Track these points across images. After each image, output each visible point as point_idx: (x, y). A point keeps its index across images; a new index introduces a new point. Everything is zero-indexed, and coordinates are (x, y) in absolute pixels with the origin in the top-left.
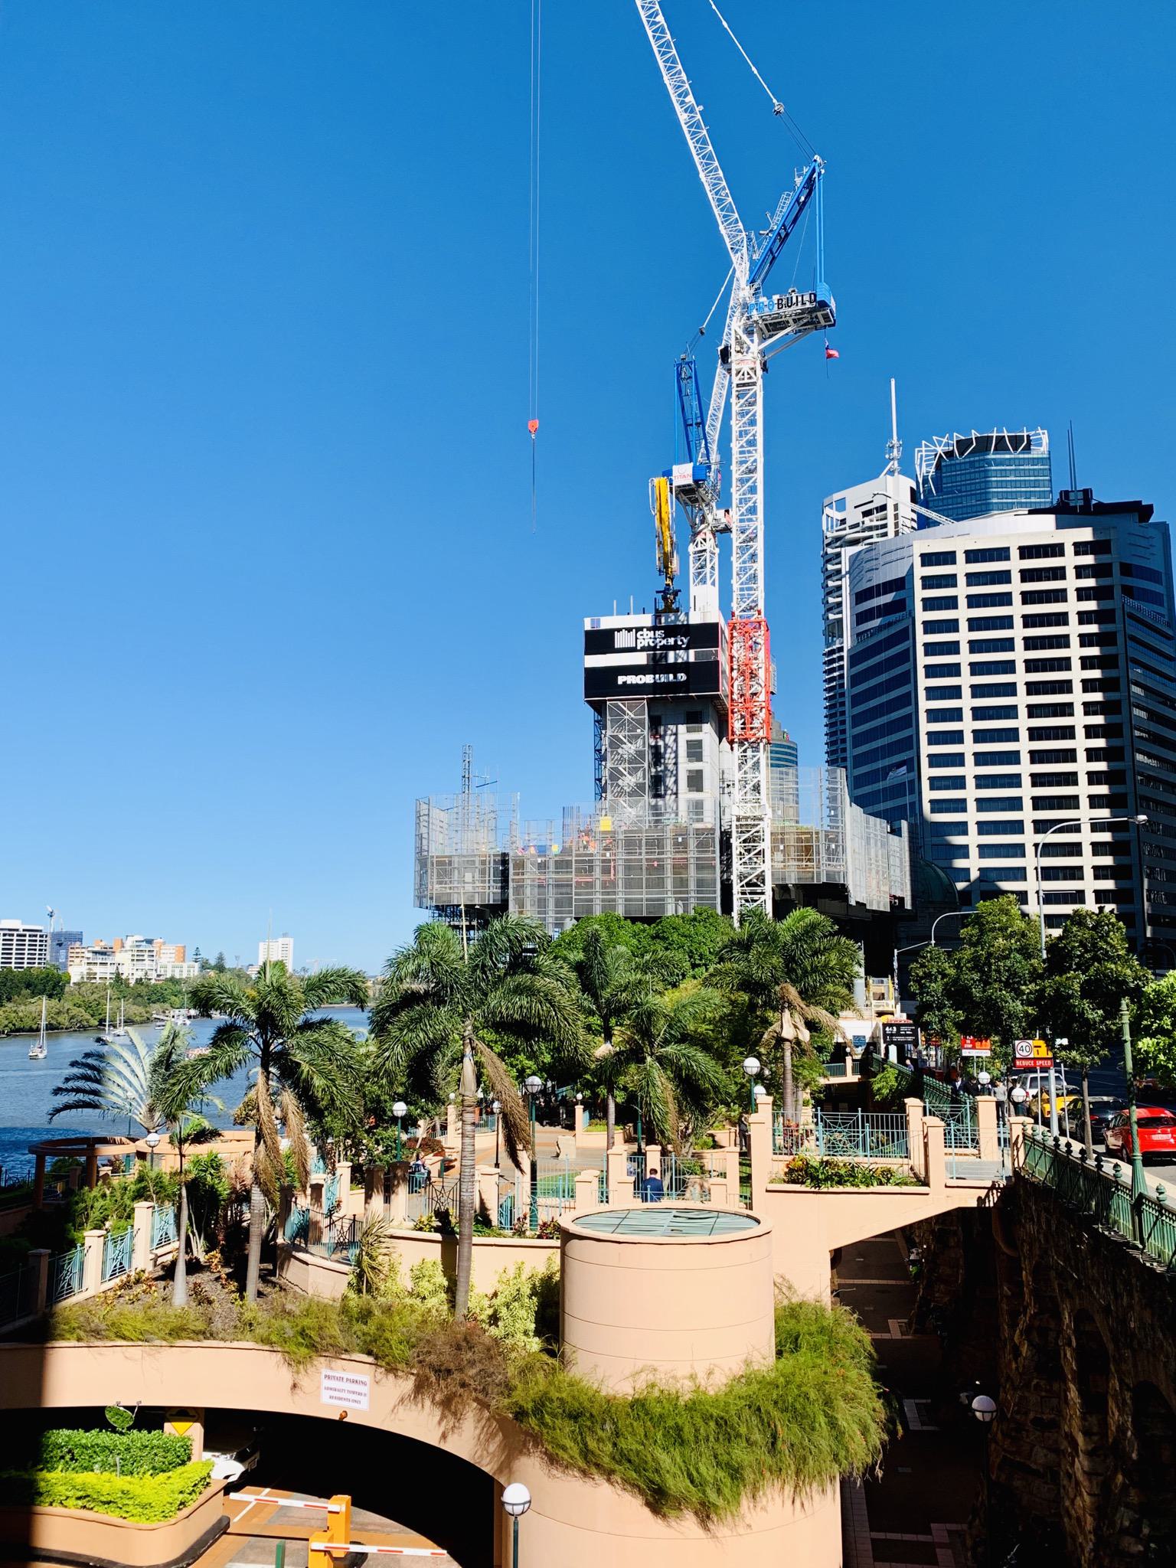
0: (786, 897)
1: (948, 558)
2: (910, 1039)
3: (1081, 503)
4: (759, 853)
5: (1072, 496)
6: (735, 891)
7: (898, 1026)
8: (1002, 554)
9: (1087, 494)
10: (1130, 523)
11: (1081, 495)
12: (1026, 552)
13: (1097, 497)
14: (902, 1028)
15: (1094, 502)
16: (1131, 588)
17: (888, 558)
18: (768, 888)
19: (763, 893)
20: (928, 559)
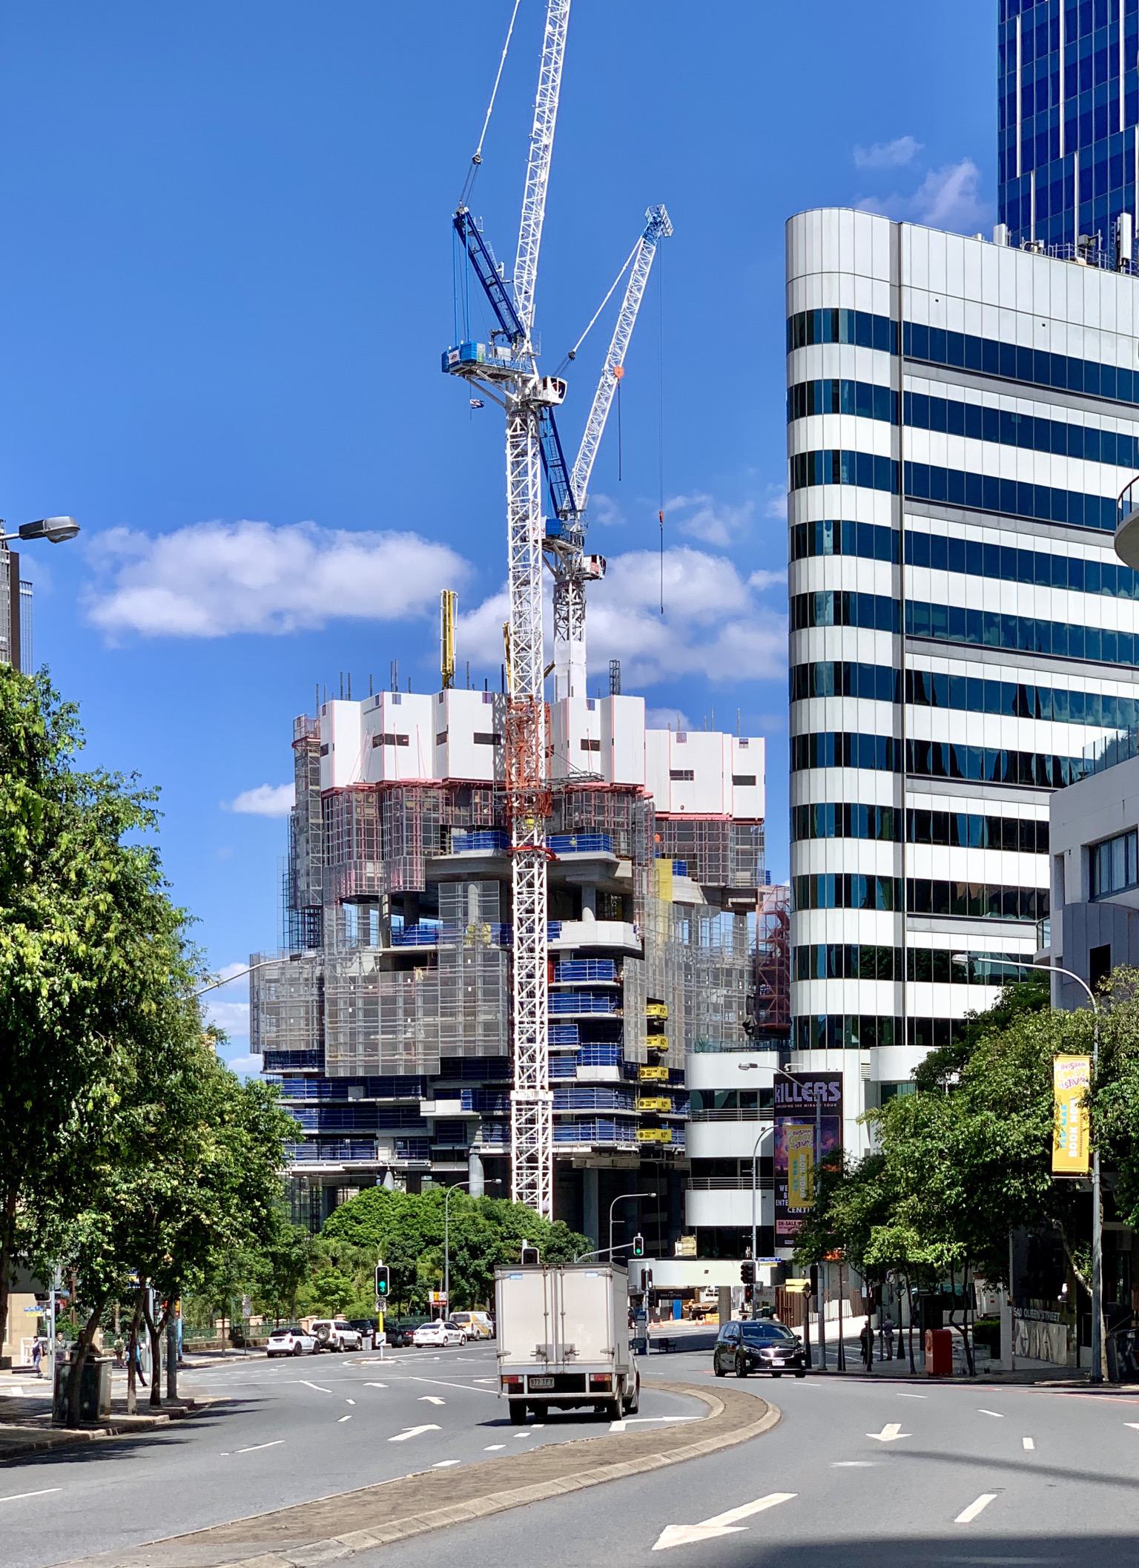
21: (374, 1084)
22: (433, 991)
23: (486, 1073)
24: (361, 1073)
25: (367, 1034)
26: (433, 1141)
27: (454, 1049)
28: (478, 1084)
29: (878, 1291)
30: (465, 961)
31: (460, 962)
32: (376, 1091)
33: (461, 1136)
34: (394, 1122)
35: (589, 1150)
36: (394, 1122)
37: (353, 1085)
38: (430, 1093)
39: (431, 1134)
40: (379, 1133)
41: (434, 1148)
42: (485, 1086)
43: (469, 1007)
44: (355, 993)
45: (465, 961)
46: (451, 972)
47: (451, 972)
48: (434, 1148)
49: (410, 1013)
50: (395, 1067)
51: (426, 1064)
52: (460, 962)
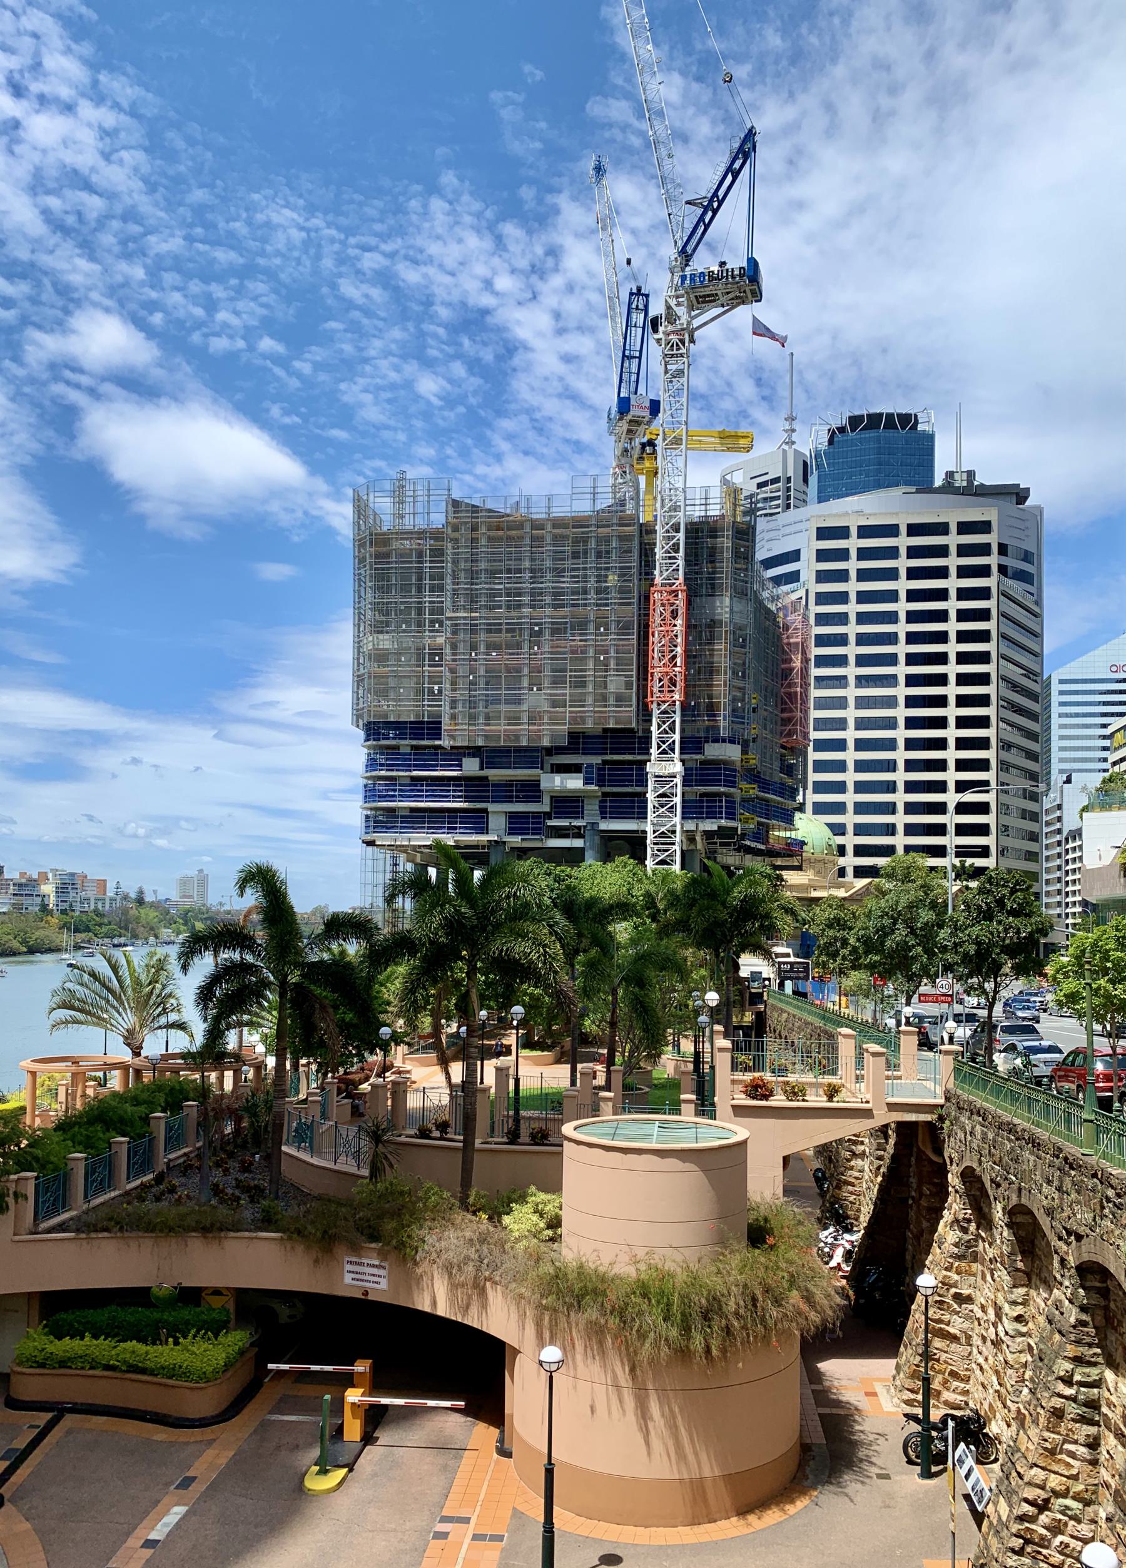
0: (692, 847)
1: (842, 532)
2: (801, 975)
3: (965, 484)
4: (672, 807)
5: (957, 476)
6: (648, 842)
7: (792, 964)
8: (891, 530)
9: (971, 474)
10: (1009, 505)
11: (965, 476)
12: (914, 530)
13: (979, 480)
14: (796, 966)
15: (976, 483)
16: (1006, 567)
17: (788, 530)
18: (678, 838)
19: (674, 844)
20: (824, 533)
21: (491, 756)
22: (562, 659)
23: (606, 749)
24: (480, 742)
25: (487, 704)
26: (548, 815)
27: (583, 720)
28: (597, 760)
29: (152, 1186)
30: (531, 648)
31: (526, 649)
32: (492, 763)
33: (578, 813)
34: (506, 797)
35: (715, 828)
36: (506, 797)
37: (469, 755)
38: (547, 767)
39: (547, 809)
40: (491, 807)
41: (550, 823)
42: (605, 762)
43: (600, 676)
44: (476, 660)
45: (531, 648)
46: (581, 640)
47: (581, 640)
48: (550, 823)
49: (535, 682)
50: (517, 738)
51: (549, 732)
52: (526, 649)
